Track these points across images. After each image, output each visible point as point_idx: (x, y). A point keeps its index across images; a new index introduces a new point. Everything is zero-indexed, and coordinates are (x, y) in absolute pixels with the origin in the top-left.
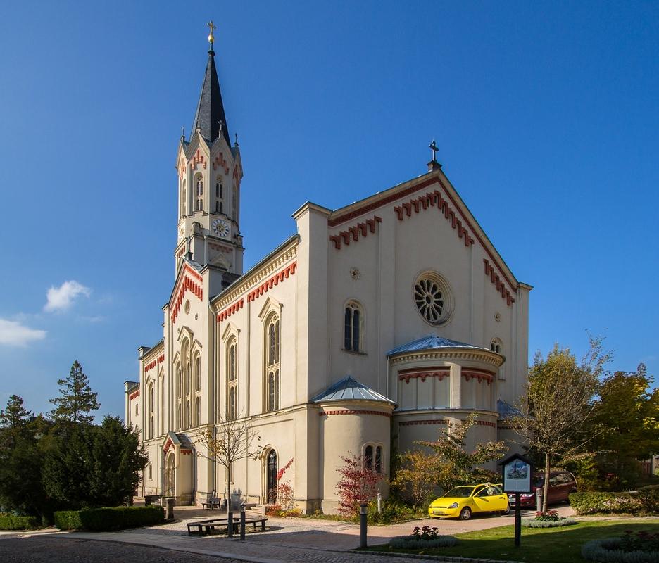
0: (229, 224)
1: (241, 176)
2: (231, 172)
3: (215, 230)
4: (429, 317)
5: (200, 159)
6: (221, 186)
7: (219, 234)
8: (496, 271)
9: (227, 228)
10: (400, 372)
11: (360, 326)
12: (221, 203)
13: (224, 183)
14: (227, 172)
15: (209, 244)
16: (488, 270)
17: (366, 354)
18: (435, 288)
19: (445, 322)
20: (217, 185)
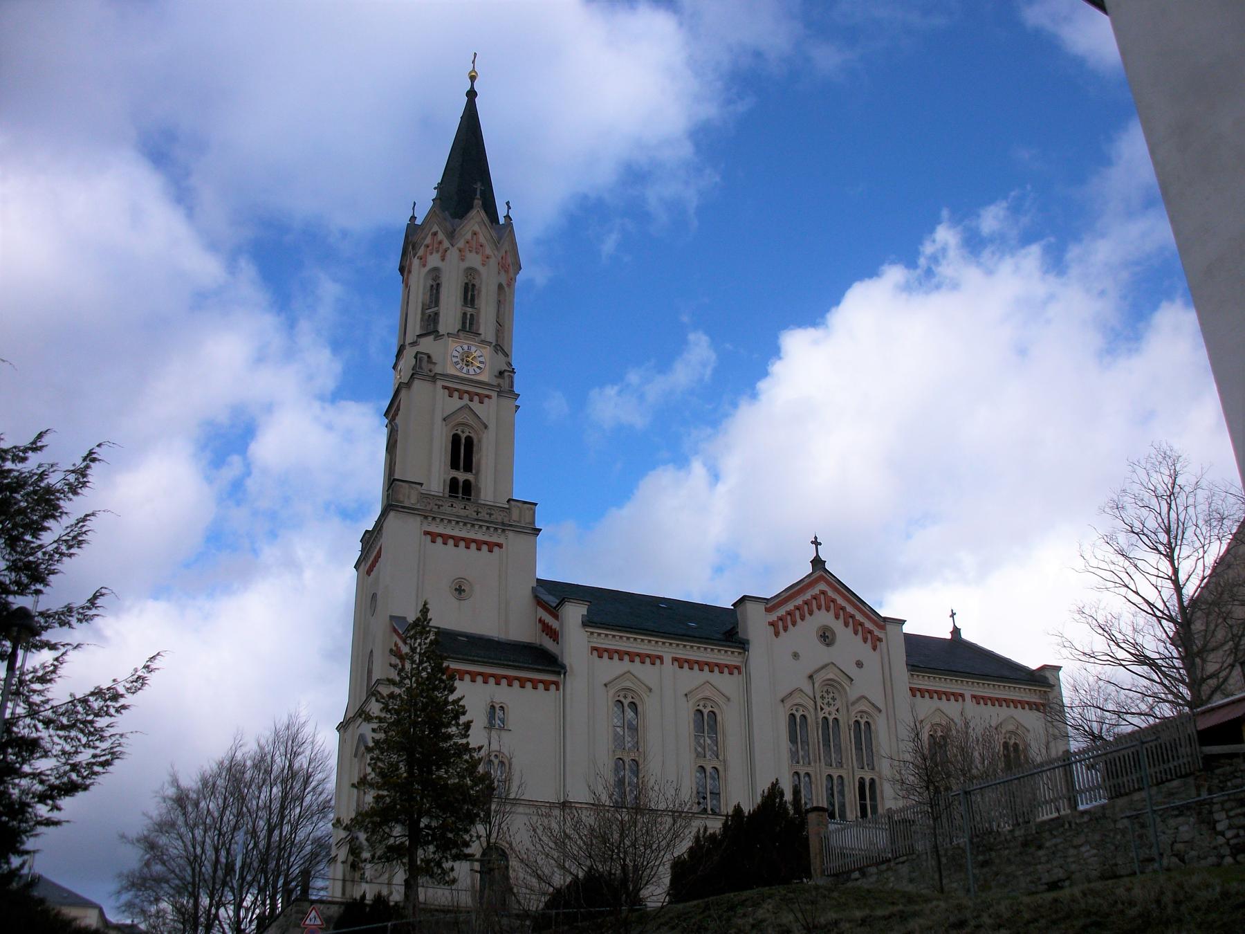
0: (487, 352)
2: (493, 262)
3: (457, 363)
7: (465, 371)
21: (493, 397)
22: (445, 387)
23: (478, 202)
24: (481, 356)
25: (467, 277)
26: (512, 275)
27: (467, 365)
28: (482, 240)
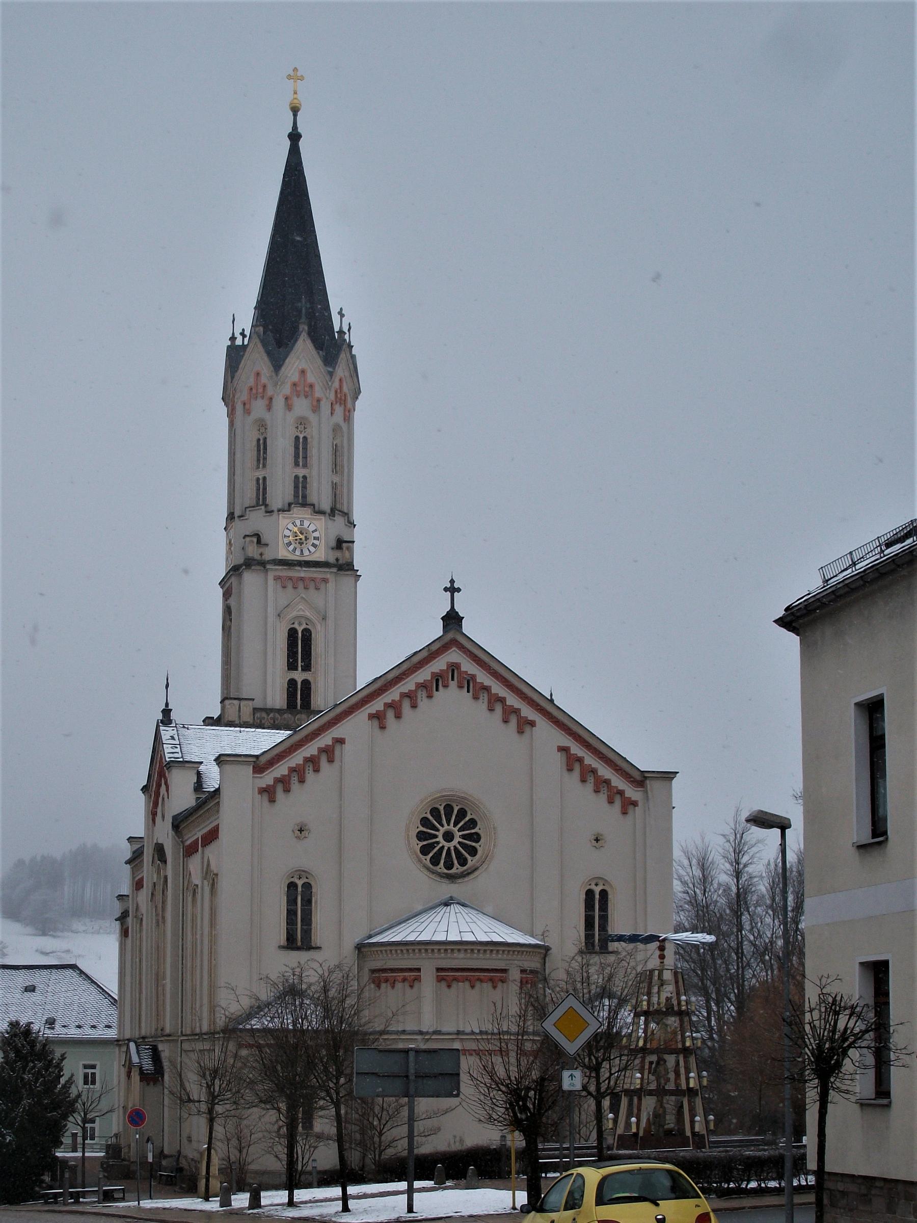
1: (357, 392)
2: (325, 407)
4: (448, 865)
5: (260, 390)
6: (305, 438)
8: (590, 760)
9: (316, 534)
10: (373, 971)
11: (313, 904)
12: (305, 477)
13: (312, 433)
14: (316, 408)
15: (277, 578)
16: (572, 762)
17: (319, 948)
18: (462, 813)
19: (476, 869)
20: (297, 438)
21: (330, 581)
23: (303, 328)
24: (316, 530)
25: (297, 428)
26: (349, 405)
28: (310, 378)
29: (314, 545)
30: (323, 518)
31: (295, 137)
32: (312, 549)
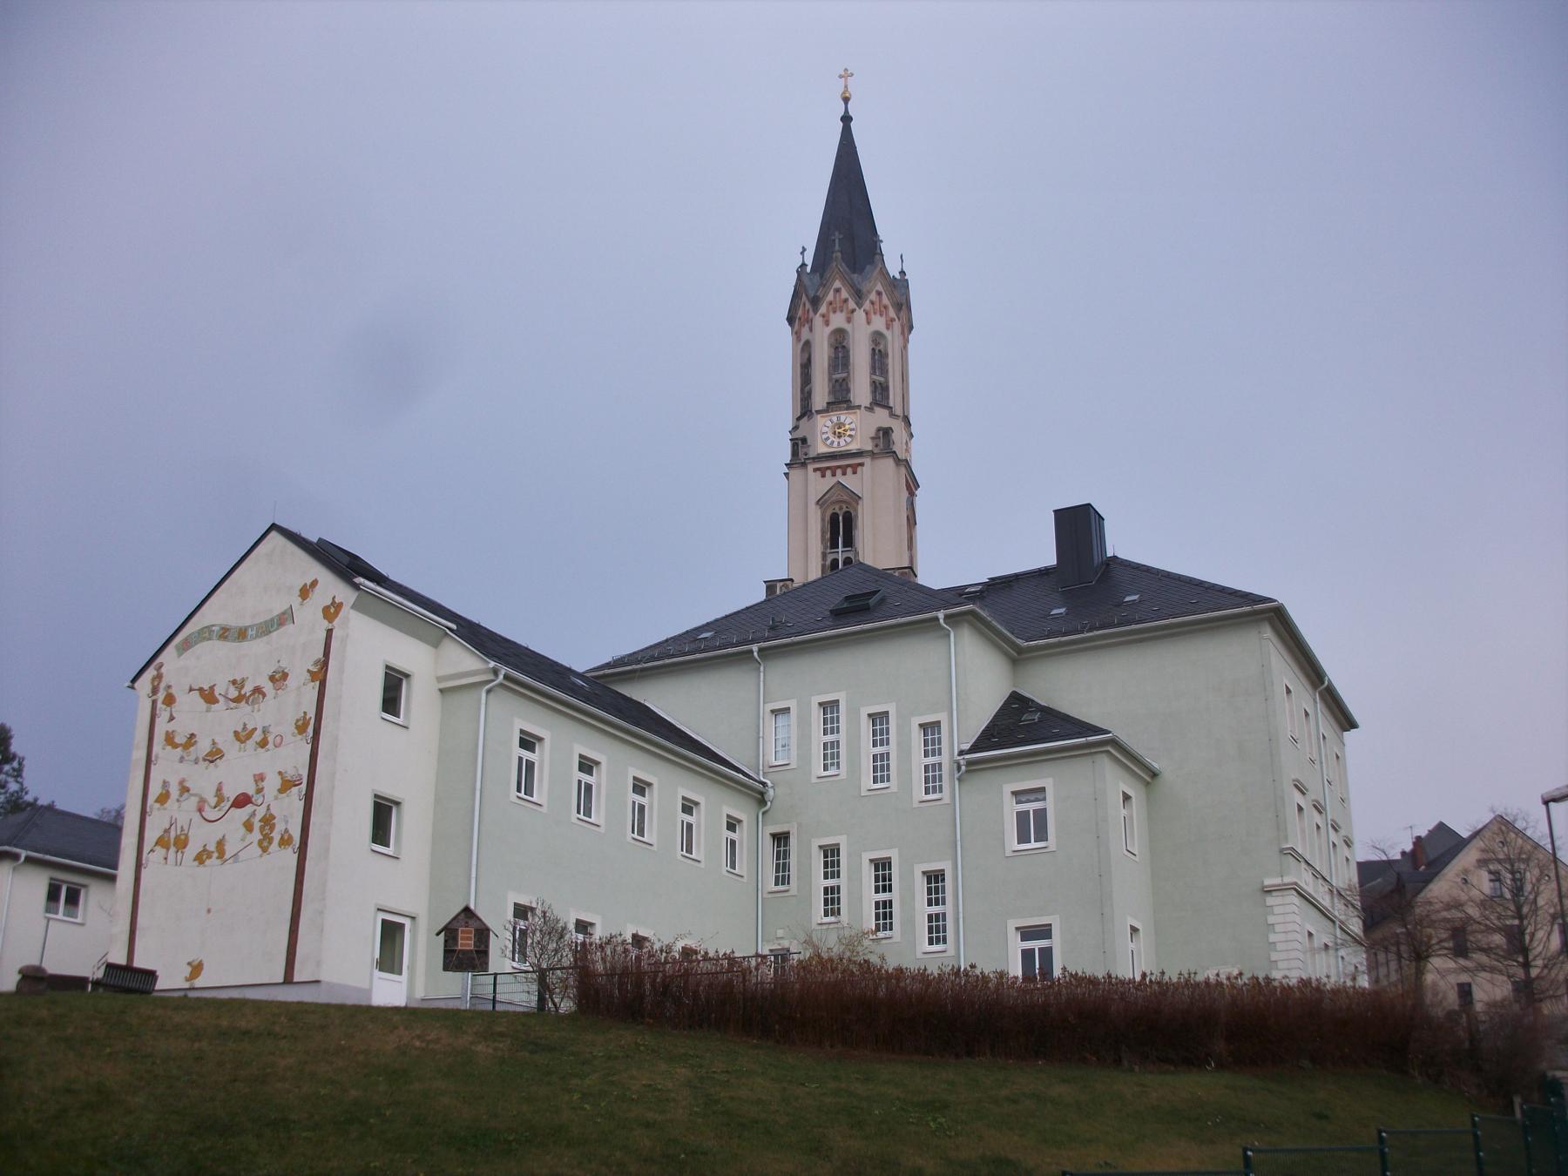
3: (828, 438)
7: (835, 444)
9: (853, 426)
22: (815, 470)
27: (839, 437)
29: (850, 436)
30: (858, 411)
31: (846, 119)
32: (848, 439)
